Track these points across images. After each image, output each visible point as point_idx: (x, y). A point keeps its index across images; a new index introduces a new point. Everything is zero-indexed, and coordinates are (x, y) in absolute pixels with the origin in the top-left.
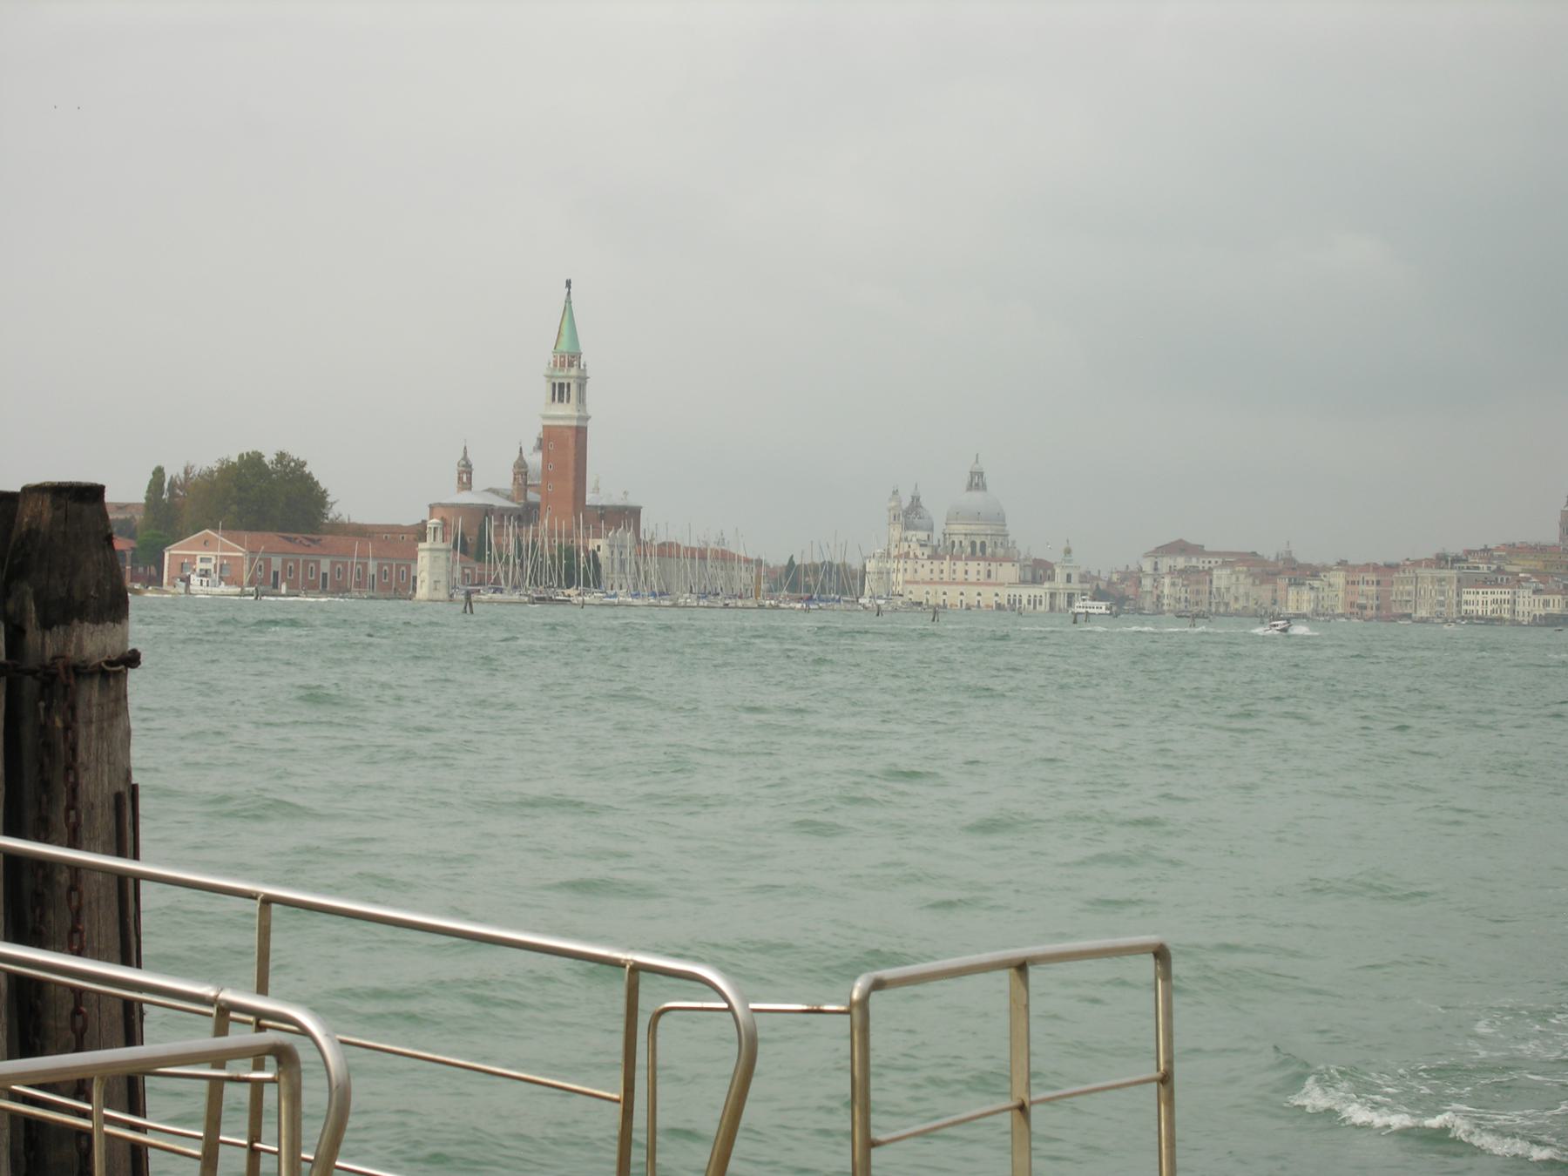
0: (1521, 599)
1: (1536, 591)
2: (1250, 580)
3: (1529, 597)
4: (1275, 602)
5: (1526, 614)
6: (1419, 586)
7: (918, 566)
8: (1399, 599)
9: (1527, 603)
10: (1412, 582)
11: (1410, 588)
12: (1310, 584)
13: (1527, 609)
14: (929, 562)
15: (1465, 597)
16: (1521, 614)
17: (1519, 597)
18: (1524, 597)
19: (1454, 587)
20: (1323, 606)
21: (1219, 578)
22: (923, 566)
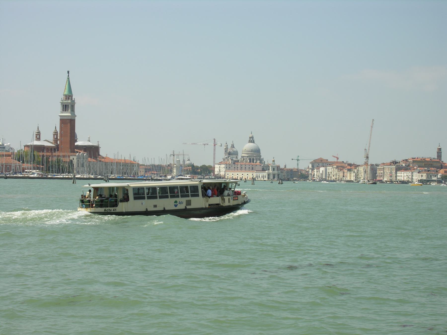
0: (414, 175)
1: (419, 172)
2: (337, 170)
3: (417, 174)
4: (344, 177)
5: (416, 179)
6: (385, 171)
7: (230, 166)
8: (379, 175)
9: (416, 176)
10: (382, 170)
11: (382, 172)
12: (354, 171)
13: (416, 178)
14: (234, 165)
15: (398, 174)
16: (414, 179)
17: (414, 174)
18: (415, 174)
19: (395, 171)
20: (357, 178)
21: (329, 169)
22: (232, 166)
